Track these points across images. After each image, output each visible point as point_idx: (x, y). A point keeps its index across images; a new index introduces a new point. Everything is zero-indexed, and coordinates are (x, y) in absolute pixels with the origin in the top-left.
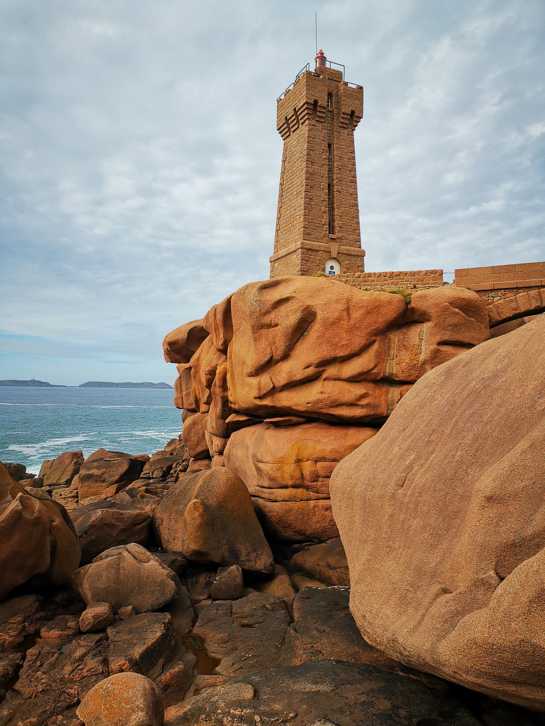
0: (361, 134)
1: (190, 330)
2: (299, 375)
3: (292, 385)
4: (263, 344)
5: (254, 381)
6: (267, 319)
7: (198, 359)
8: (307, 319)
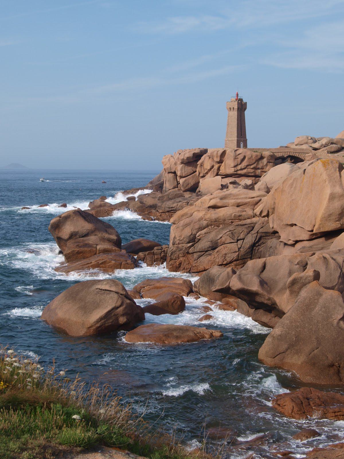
0: (246, 112)
1: (193, 154)
2: (243, 168)
3: (241, 169)
4: (236, 161)
5: (233, 169)
6: (237, 157)
7: (203, 162)
8: (244, 157)
